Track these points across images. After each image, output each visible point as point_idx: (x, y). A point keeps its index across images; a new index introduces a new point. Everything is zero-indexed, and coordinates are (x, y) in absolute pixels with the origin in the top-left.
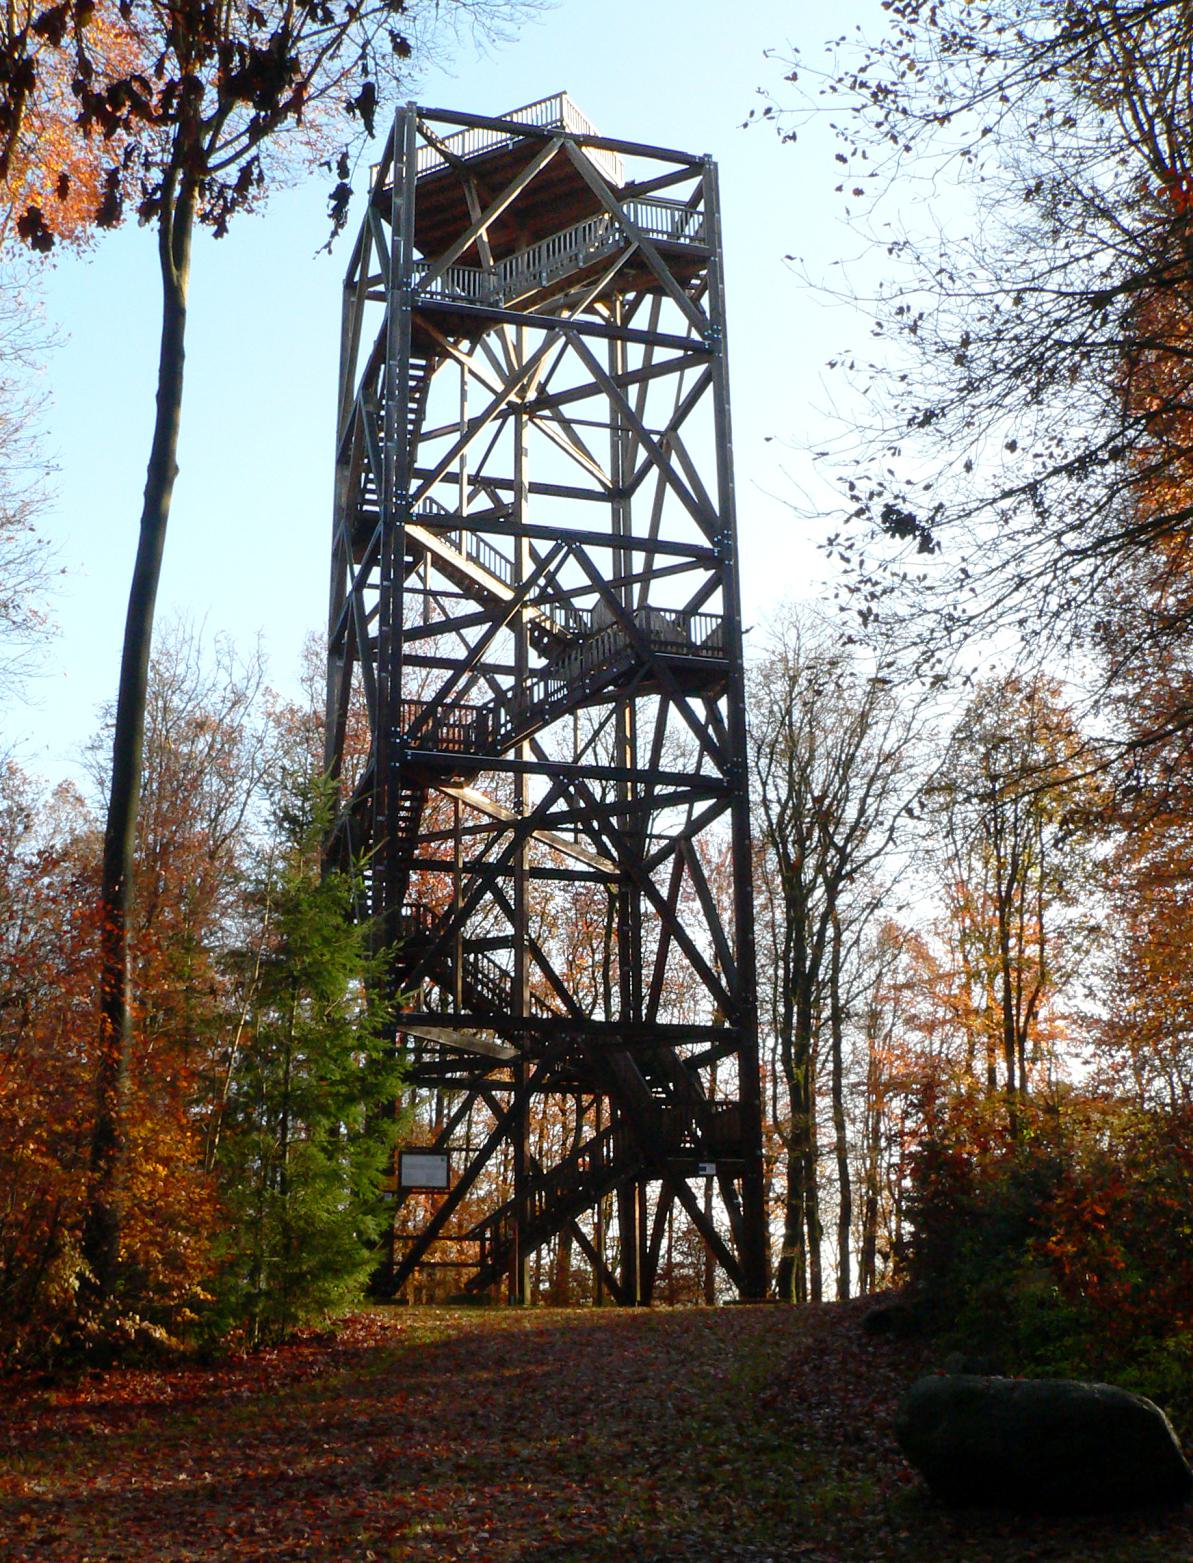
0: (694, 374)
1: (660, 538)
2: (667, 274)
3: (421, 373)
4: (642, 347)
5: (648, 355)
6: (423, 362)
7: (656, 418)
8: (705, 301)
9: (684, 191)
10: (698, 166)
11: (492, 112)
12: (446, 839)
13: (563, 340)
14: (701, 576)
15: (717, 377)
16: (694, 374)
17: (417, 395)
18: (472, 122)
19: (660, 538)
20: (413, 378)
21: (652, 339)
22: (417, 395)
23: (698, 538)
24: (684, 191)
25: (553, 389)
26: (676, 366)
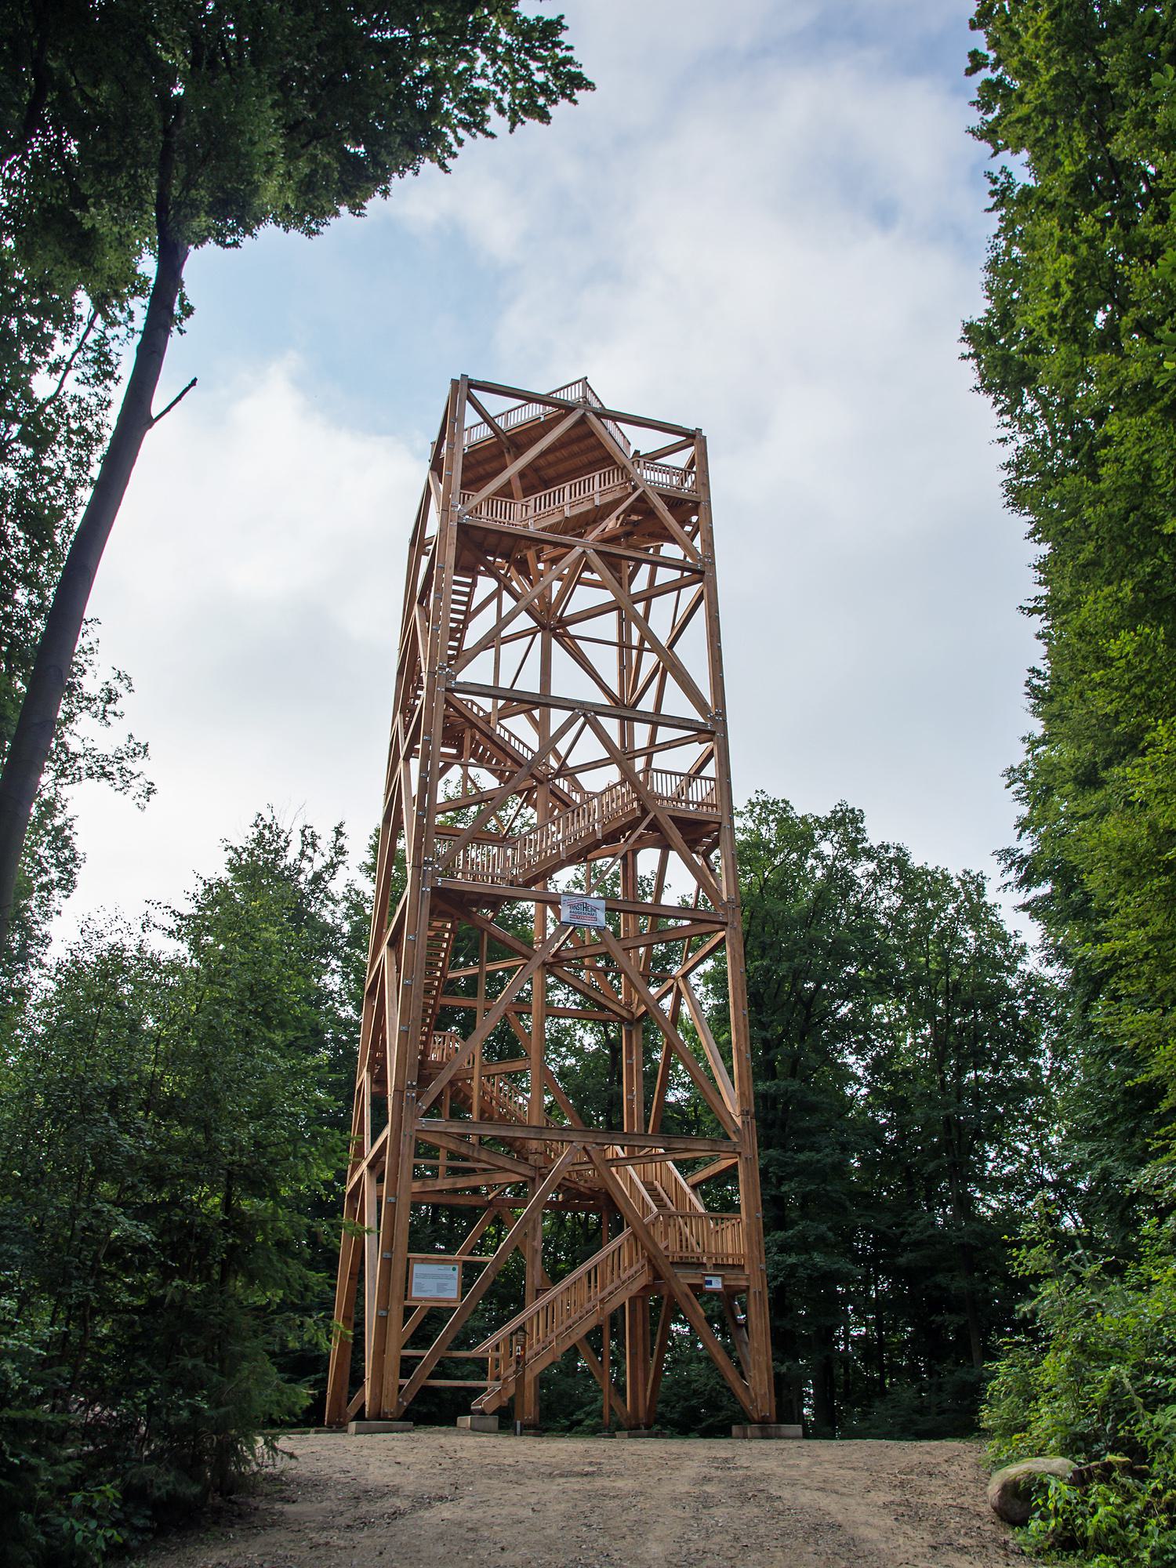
0: (689, 594)
1: (659, 851)
2: (675, 835)
3: (461, 617)
4: (648, 727)
5: (653, 576)
6: (469, 580)
7: (660, 626)
8: (697, 542)
9: (680, 459)
10: (692, 437)
11: (543, 390)
12: (442, 826)
13: (582, 719)
14: (696, 750)
15: (709, 598)
16: (689, 594)
17: (458, 635)
18: (530, 398)
19: (659, 851)
20: (453, 620)
21: (656, 720)
22: (458, 635)
23: (692, 713)
24: (680, 459)
25: (571, 762)
26: (676, 586)
